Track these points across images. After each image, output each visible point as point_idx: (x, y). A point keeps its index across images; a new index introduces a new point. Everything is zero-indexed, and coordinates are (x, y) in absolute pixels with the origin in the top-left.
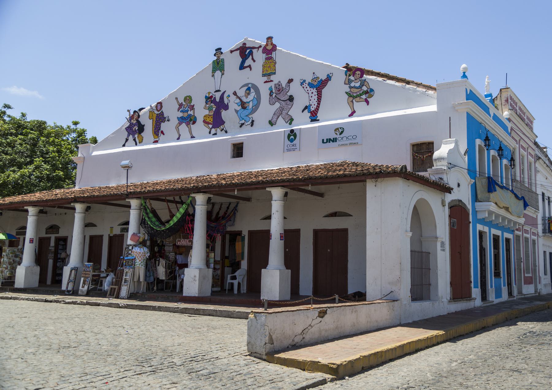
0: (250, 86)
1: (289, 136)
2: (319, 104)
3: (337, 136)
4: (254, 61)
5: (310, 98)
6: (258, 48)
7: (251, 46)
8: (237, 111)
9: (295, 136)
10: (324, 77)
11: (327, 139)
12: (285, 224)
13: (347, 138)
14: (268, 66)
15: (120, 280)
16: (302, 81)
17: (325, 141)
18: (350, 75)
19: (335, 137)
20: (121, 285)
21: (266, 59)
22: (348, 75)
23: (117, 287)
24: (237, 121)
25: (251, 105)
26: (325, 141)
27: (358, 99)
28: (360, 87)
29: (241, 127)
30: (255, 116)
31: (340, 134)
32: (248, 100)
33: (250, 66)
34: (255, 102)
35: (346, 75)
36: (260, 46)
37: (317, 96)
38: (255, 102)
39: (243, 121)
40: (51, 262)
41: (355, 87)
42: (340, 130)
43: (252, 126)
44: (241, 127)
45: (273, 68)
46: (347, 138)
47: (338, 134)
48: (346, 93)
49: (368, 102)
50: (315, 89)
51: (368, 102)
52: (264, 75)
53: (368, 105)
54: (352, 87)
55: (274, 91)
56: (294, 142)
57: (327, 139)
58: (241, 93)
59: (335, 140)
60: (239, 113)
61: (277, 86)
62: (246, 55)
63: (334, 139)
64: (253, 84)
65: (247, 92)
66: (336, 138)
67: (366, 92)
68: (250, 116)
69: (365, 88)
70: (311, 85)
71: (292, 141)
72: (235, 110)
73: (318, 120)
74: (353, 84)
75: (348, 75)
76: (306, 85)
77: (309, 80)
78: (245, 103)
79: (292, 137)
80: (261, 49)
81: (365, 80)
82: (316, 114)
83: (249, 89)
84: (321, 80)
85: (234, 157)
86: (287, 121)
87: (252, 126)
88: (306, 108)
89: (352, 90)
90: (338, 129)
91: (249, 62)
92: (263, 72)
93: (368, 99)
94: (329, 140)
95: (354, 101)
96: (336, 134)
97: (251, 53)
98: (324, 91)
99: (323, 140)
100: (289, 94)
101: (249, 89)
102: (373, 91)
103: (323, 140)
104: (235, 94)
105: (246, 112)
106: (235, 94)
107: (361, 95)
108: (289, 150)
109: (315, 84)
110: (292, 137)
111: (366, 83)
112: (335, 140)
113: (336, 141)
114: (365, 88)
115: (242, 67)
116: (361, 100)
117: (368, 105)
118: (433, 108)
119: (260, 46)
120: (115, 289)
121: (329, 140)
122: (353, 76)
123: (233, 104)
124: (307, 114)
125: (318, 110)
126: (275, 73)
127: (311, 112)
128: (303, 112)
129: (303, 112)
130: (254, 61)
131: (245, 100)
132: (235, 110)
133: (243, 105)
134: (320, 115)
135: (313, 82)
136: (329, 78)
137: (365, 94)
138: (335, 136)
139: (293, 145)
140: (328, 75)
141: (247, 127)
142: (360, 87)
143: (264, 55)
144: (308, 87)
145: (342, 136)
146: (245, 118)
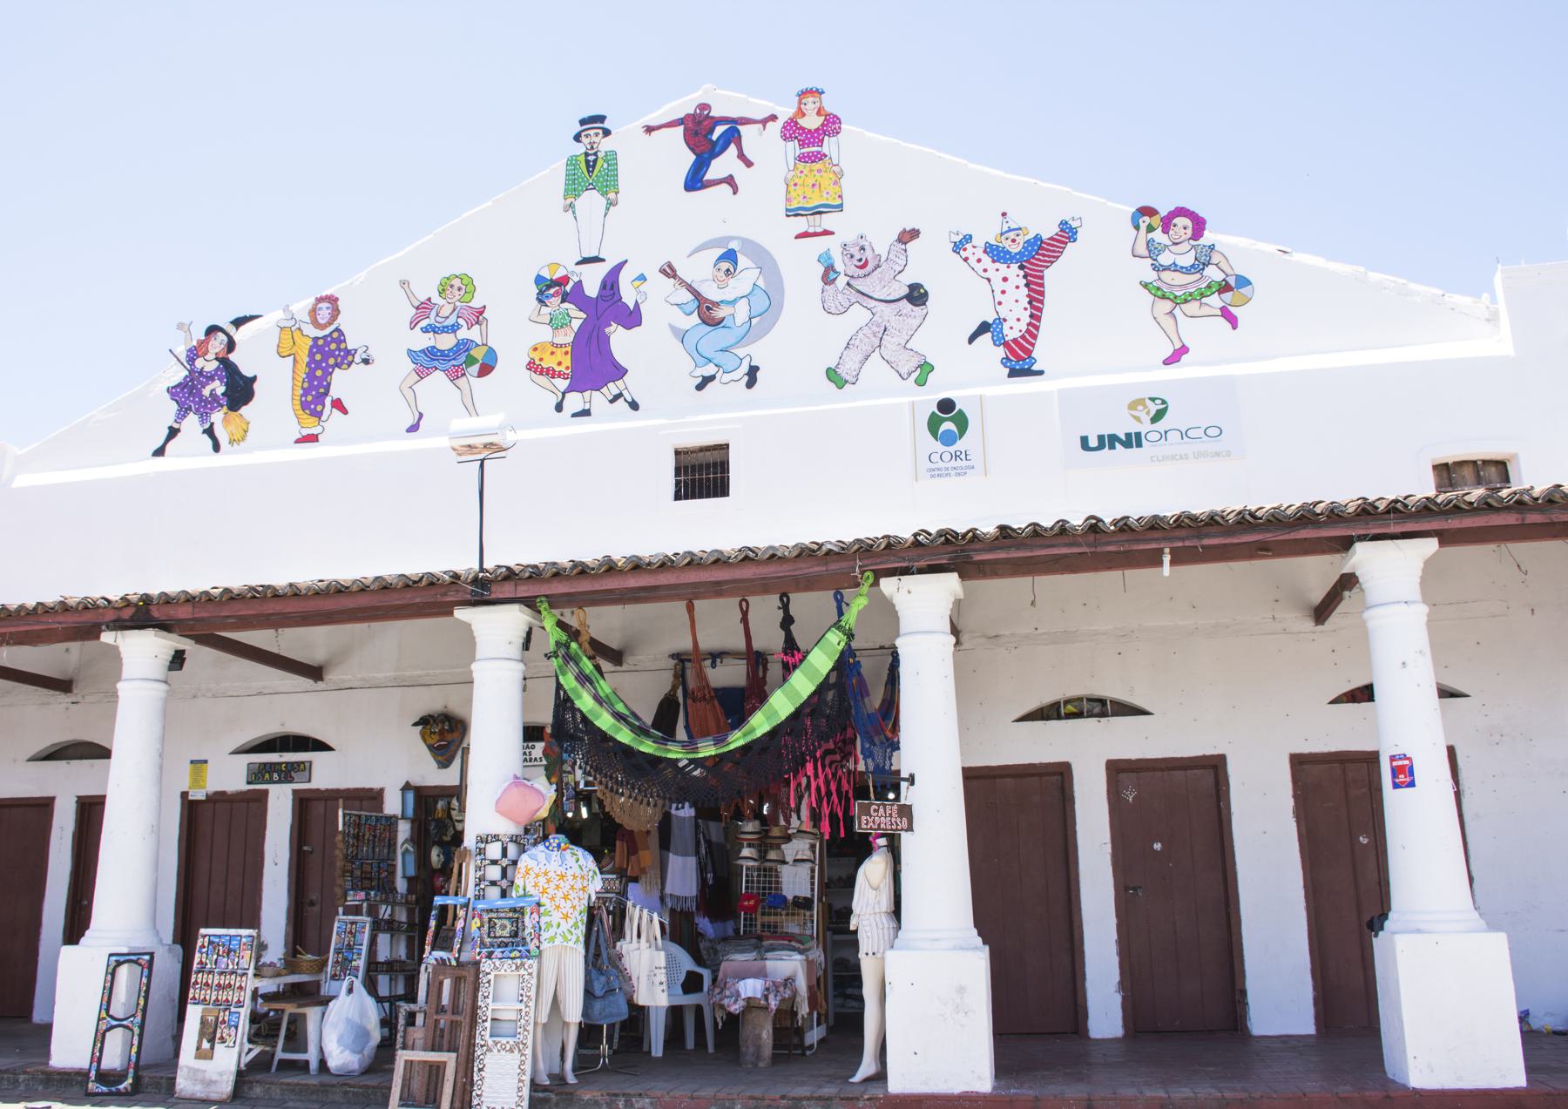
0: (733, 245)
1: (933, 425)
2: (1036, 317)
3: (1144, 427)
4: (749, 164)
5: (999, 297)
6: (764, 122)
7: (735, 115)
8: (682, 336)
9: (962, 423)
10: (1049, 230)
11: (1101, 438)
12: (963, 754)
13: (1184, 435)
14: (810, 181)
15: (465, 1020)
16: (957, 239)
17: (1093, 443)
18: (1150, 229)
19: (1133, 431)
20: (471, 1045)
21: (802, 158)
22: (1143, 227)
23: (449, 1059)
24: (685, 370)
25: (742, 312)
26: (1093, 443)
27: (1192, 307)
28: (1200, 266)
29: (700, 387)
30: (757, 352)
31: (1154, 420)
32: (728, 295)
33: (730, 180)
34: (760, 302)
35: (1137, 227)
36: (773, 118)
37: (1025, 291)
38: (760, 302)
39: (709, 370)
40: (433, 923)
41: (1174, 268)
42: (1153, 408)
43: (750, 385)
44: (700, 387)
45: (833, 190)
46: (1184, 435)
47: (1147, 419)
48: (1146, 286)
49: (1233, 321)
50: (1015, 267)
51: (1233, 321)
52: (793, 213)
53: (1235, 327)
54: (1167, 269)
55: (839, 266)
56: (960, 445)
57: (1101, 438)
58: (700, 270)
59: (1133, 441)
60: (691, 340)
61: (855, 251)
62: (714, 144)
63: (1128, 435)
64: (744, 241)
65: (725, 265)
66: (1138, 435)
67: (1225, 288)
68: (741, 352)
69: (1213, 274)
70: (997, 253)
71: (948, 440)
72: (674, 329)
73: (1041, 373)
74: (1165, 259)
75: (1143, 227)
76: (974, 252)
77: (986, 233)
78: (717, 304)
79: (948, 426)
80: (775, 128)
81: (1212, 247)
82: (1029, 353)
83: (730, 256)
84: (1037, 238)
85: (677, 497)
86: (904, 371)
87: (750, 385)
88: (984, 328)
89: (1166, 276)
90: (1141, 402)
91: (719, 167)
92: (788, 200)
93: (1232, 310)
94: (1109, 441)
95: (1177, 311)
96: (1138, 419)
97: (733, 136)
98: (1053, 276)
99: (1084, 440)
100: (908, 278)
101: (730, 256)
102: (1249, 283)
103: (1084, 440)
104: (669, 271)
105: (718, 337)
106: (669, 271)
107: (1203, 295)
108: (935, 473)
109: (1015, 249)
110: (948, 426)
111: (1216, 258)
112: (1133, 441)
113: (1139, 445)
114: (1213, 274)
115: (695, 181)
116: (1205, 311)
117: (1235, 327)
118: (1498, 343)
119: (773, 118)
120: (436, 1070)
121: (1109, 441)
122: (1166, 230)
123: (662, 308)
124: (989, 353)
125: (1035, 337)
126: (840, 207)
127: (1006, 344)
128: (972, 339)
129: (972, 339)
130: (749, 164)
131: (711, 293)
132: (674, 329)
133: (707, 312)
134: (1042, 354)
135: (1007, 244)
136: (1067, 233)
137: (1220, 291)
138: (1133, 428)
139: (956, 456)
140: (1063, 223)
141: (729, 388)
142: (1200, 266)
143: (793, 148)
144: (987, 260)
145: (1161, 425)
146: (721, 358)
